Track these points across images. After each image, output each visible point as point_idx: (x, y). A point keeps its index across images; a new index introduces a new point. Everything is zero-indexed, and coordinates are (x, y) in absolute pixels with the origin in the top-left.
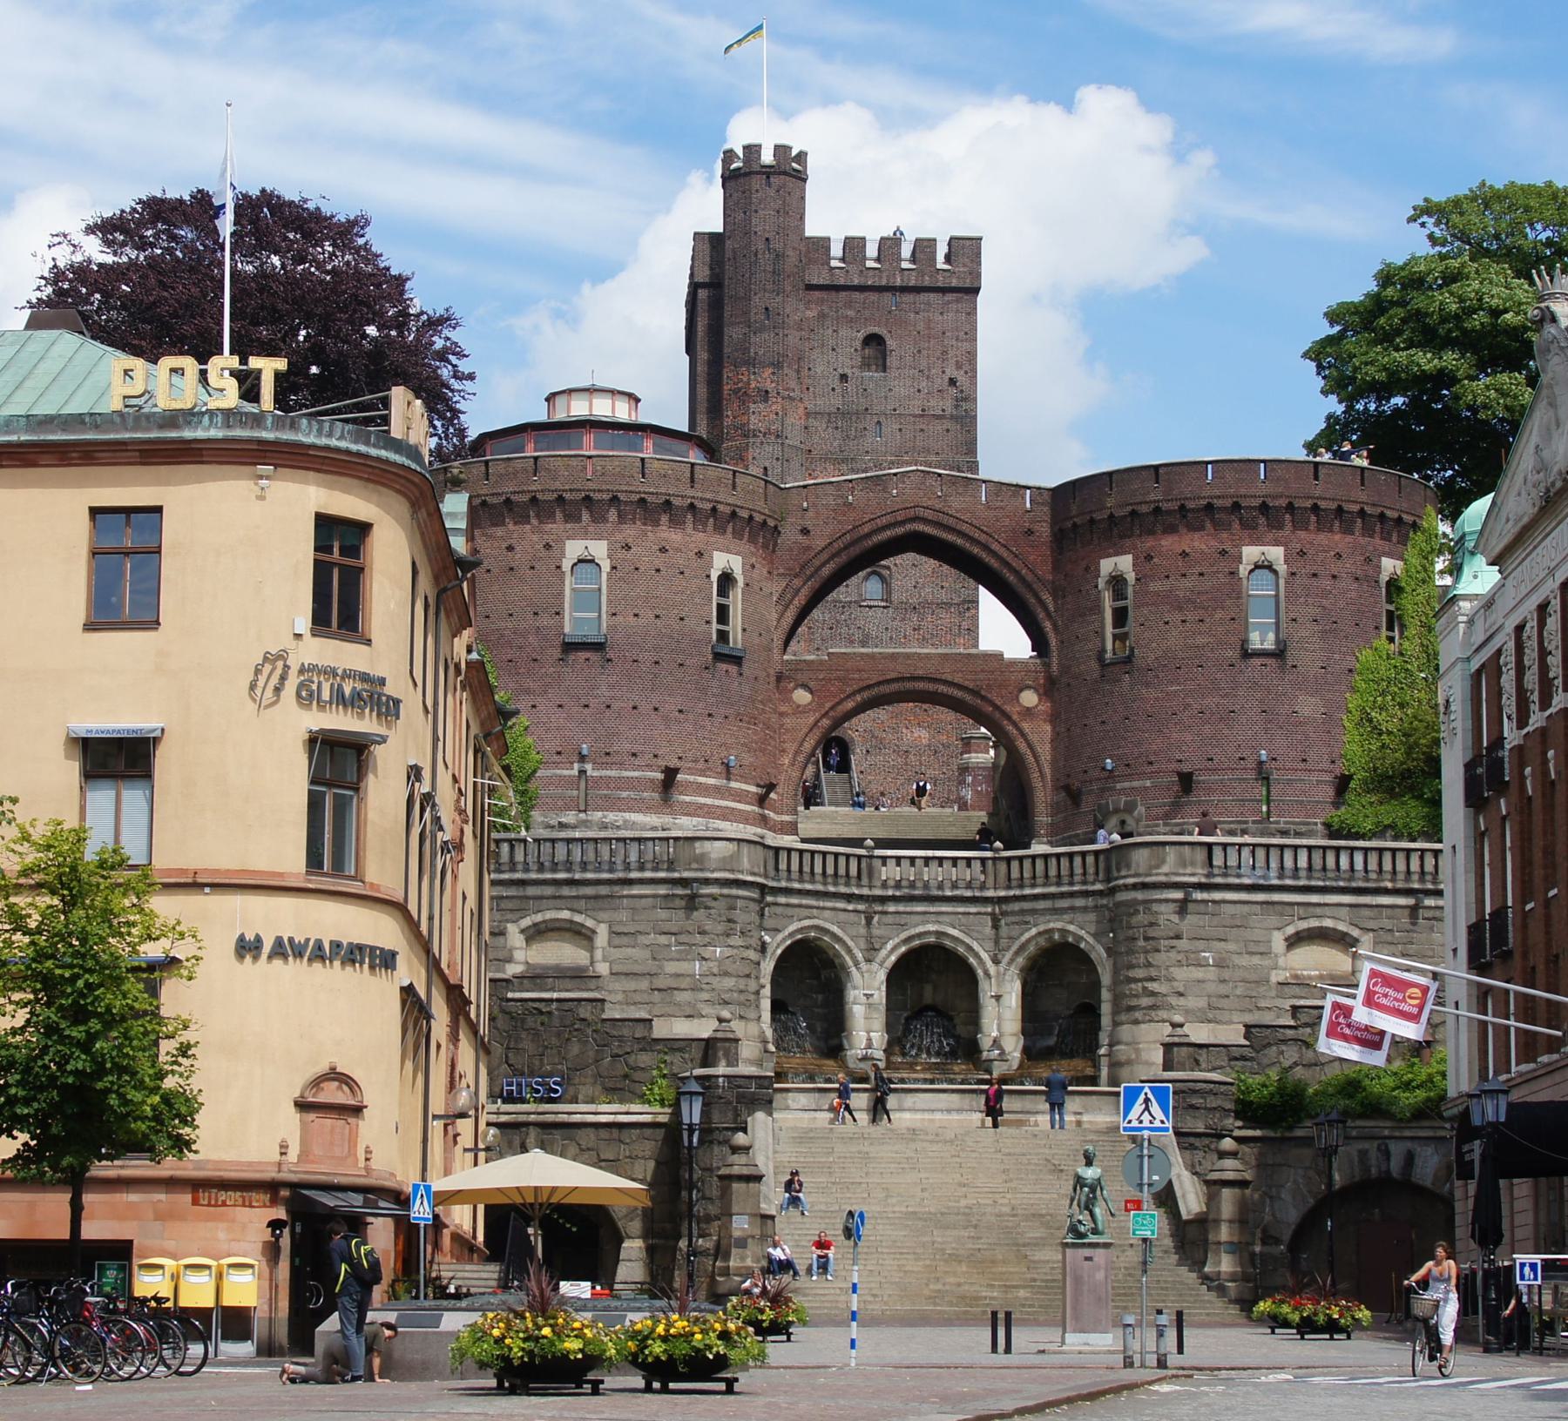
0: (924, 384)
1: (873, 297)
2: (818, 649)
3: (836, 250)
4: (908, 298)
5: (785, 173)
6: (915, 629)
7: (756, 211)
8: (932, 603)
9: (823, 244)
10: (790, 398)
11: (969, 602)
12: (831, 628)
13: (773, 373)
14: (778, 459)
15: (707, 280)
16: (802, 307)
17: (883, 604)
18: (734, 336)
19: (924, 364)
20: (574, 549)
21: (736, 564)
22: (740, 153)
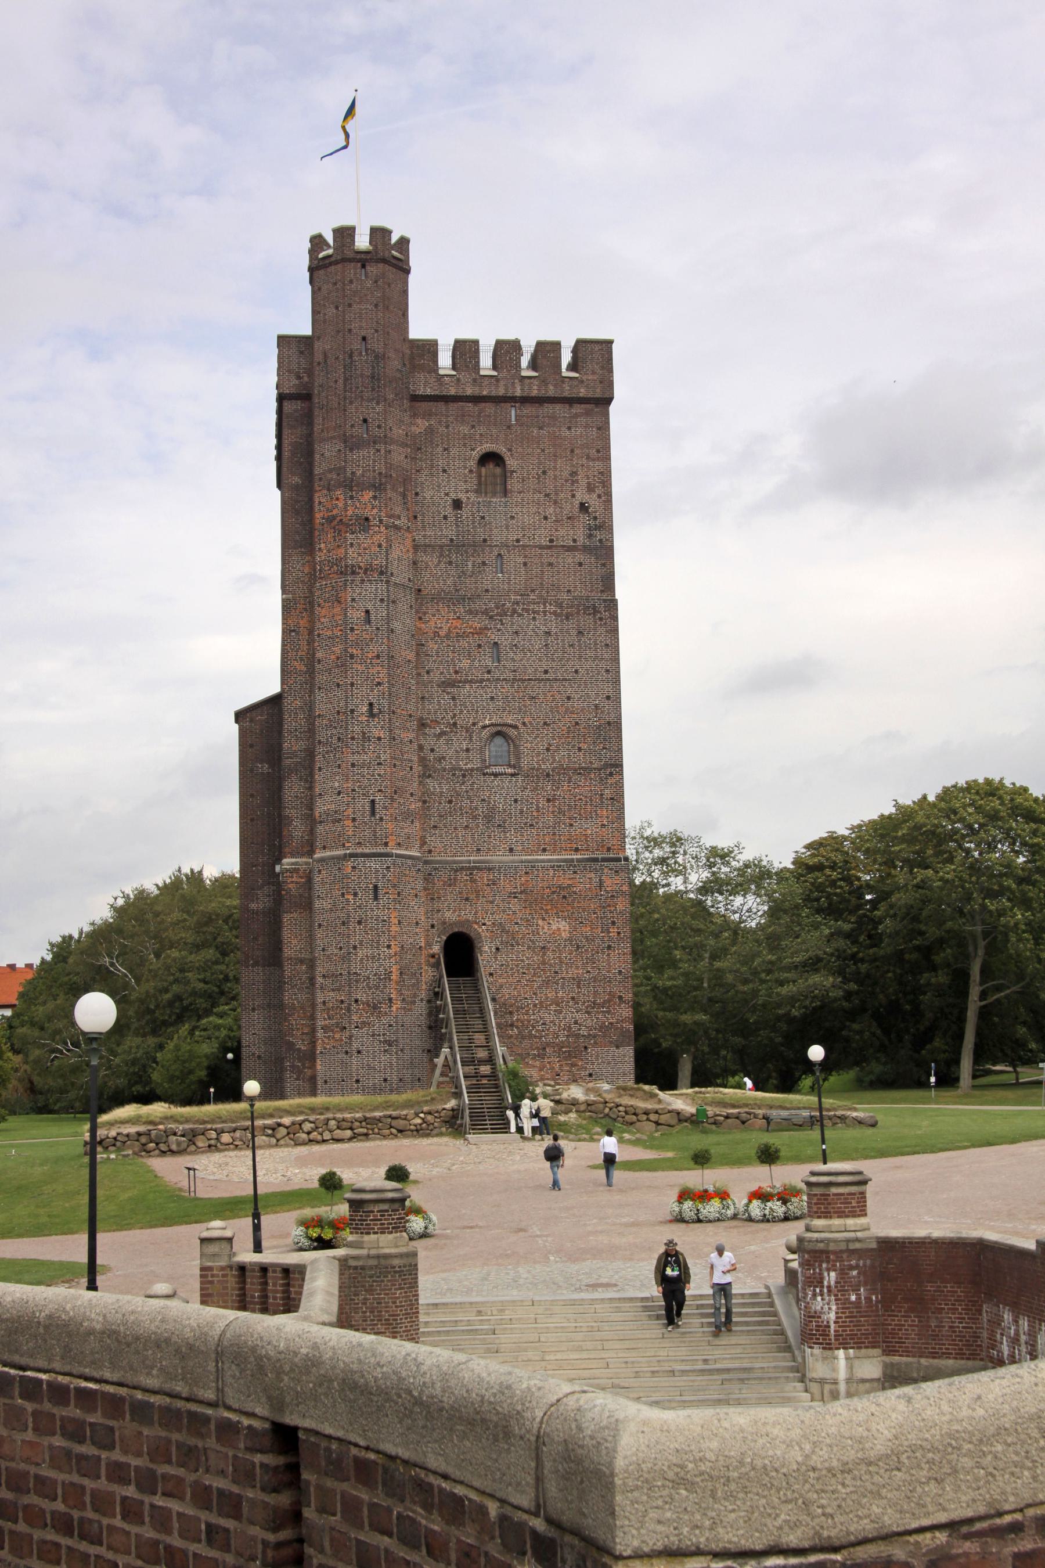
0: (551, 510)
1: (489, 408)
2: (435, 827)
3: (445, 360)
4: (528, 410)
5: (384, 261)
6: (549, 800)
7: (350, 305)
8: (569, 768)
9: (430, 348)
10: (397, 528)
11: (612, 766)
12: (450, 802)
13: (375, 497)
14: (382, 600)
15: (293, 391)
16: (407, 419)
17: (510, 771)
18: (327, 454)
19: (550, 488)
22: (330, 239)
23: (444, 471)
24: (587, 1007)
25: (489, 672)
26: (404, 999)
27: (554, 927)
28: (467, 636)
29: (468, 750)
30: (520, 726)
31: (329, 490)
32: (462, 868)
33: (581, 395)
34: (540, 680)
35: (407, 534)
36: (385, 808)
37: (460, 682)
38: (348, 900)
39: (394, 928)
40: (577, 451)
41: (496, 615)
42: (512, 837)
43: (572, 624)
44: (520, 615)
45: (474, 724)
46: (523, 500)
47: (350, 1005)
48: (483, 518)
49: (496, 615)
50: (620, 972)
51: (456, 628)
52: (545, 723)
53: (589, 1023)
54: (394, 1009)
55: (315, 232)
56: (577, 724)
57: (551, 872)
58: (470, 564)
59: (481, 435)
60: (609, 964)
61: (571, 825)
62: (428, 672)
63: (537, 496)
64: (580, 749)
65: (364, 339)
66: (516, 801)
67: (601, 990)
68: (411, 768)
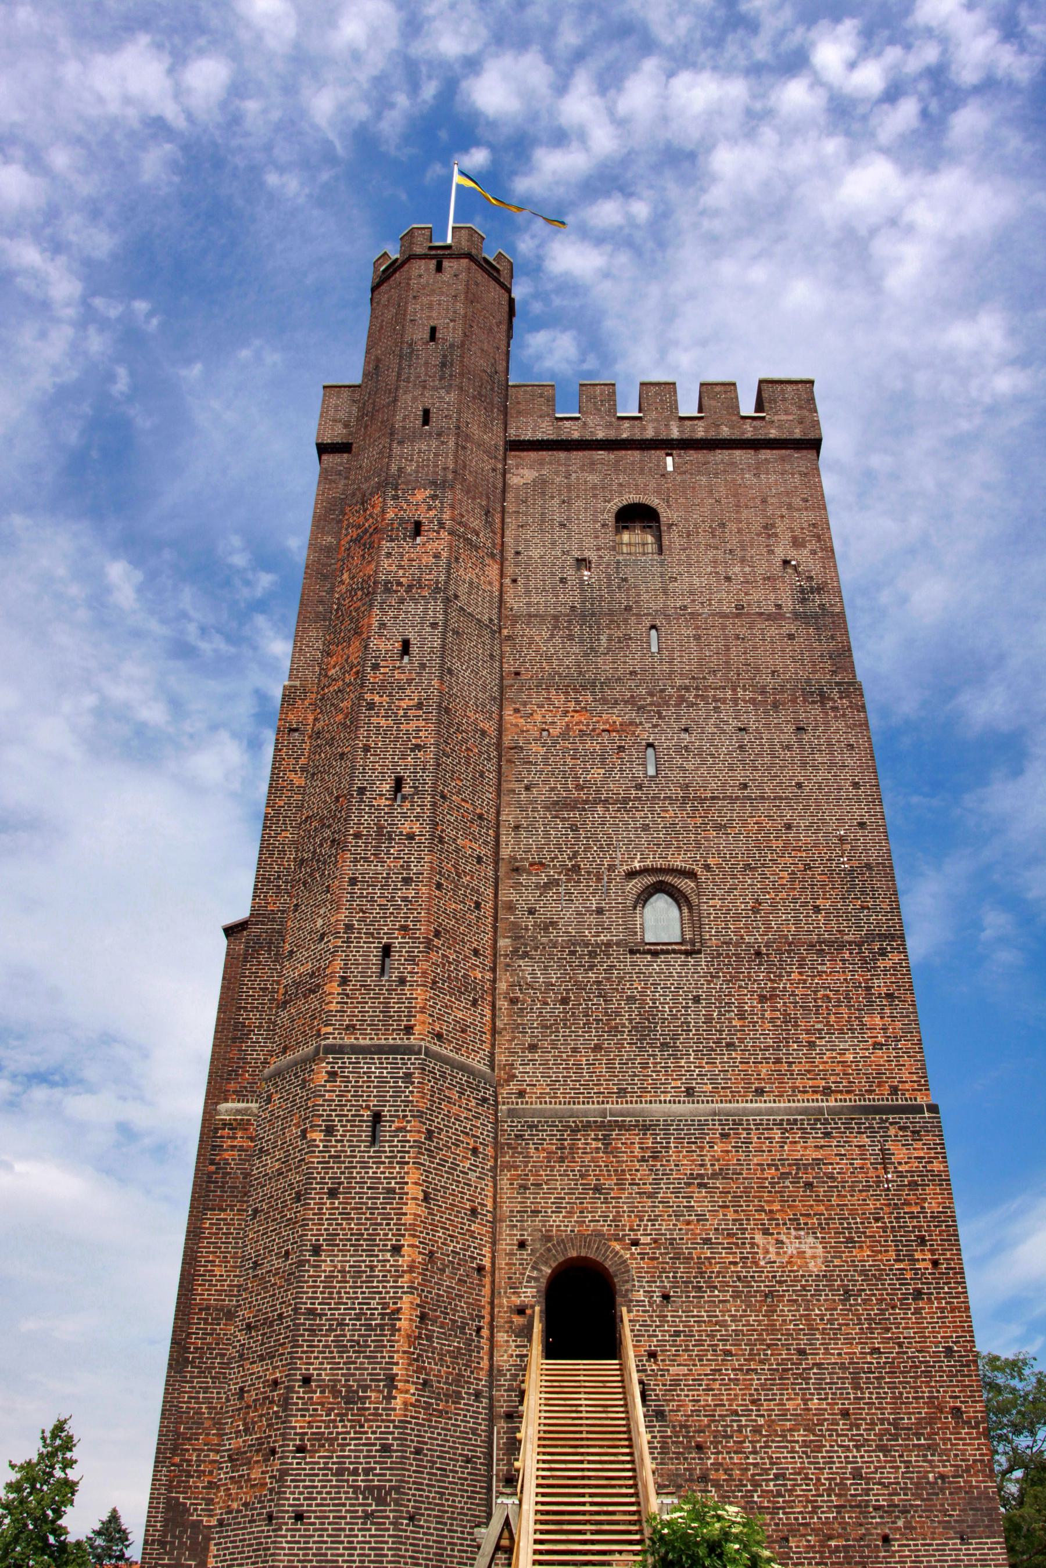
0: (737, 569)
2: (533, 1048)
4: (692, 456)
6: (762, 999)
11: (883, 937)
13: (434, 497)
14: (434, 625)
19: (734, 542)
23: (563, 525)
24: (880, 1436)
25: (639, 787)
26: (426, 1383)
27: (791, 1250)
28: (599, 735)
29: (600, 911)
30: (699, 871)
31: (363, 504)
32: (587, 1126)
33: (772, 436)
34: (733, 799)
35: (487, 561)
36: (412, 960)
37: (586, 802)
38: (312, 1144)
39: (410, 1208)
40: (770, 500)
41: (651, 704)
43: (784, 719)
44: (693, 704)
45: (611, 868)
46: (688, 556)
47: (290, 1389)
48: (625, 580)
49: (651, 704)
50: (949, 1351)
51: (577, 724)
52: (747, 867)
53: (889, 1475)
54: (398, 1403)
56: (807, 867)
57: (777, 1134)
58: (604, 638)
59: (620, 485)
60: (921, 1332)
62: (527, 788)
63: (711, 554)
64: (817, 909)
65: (433, 330)
66: (697, 1000)
67: (908, 1394)
68: (478, 906)
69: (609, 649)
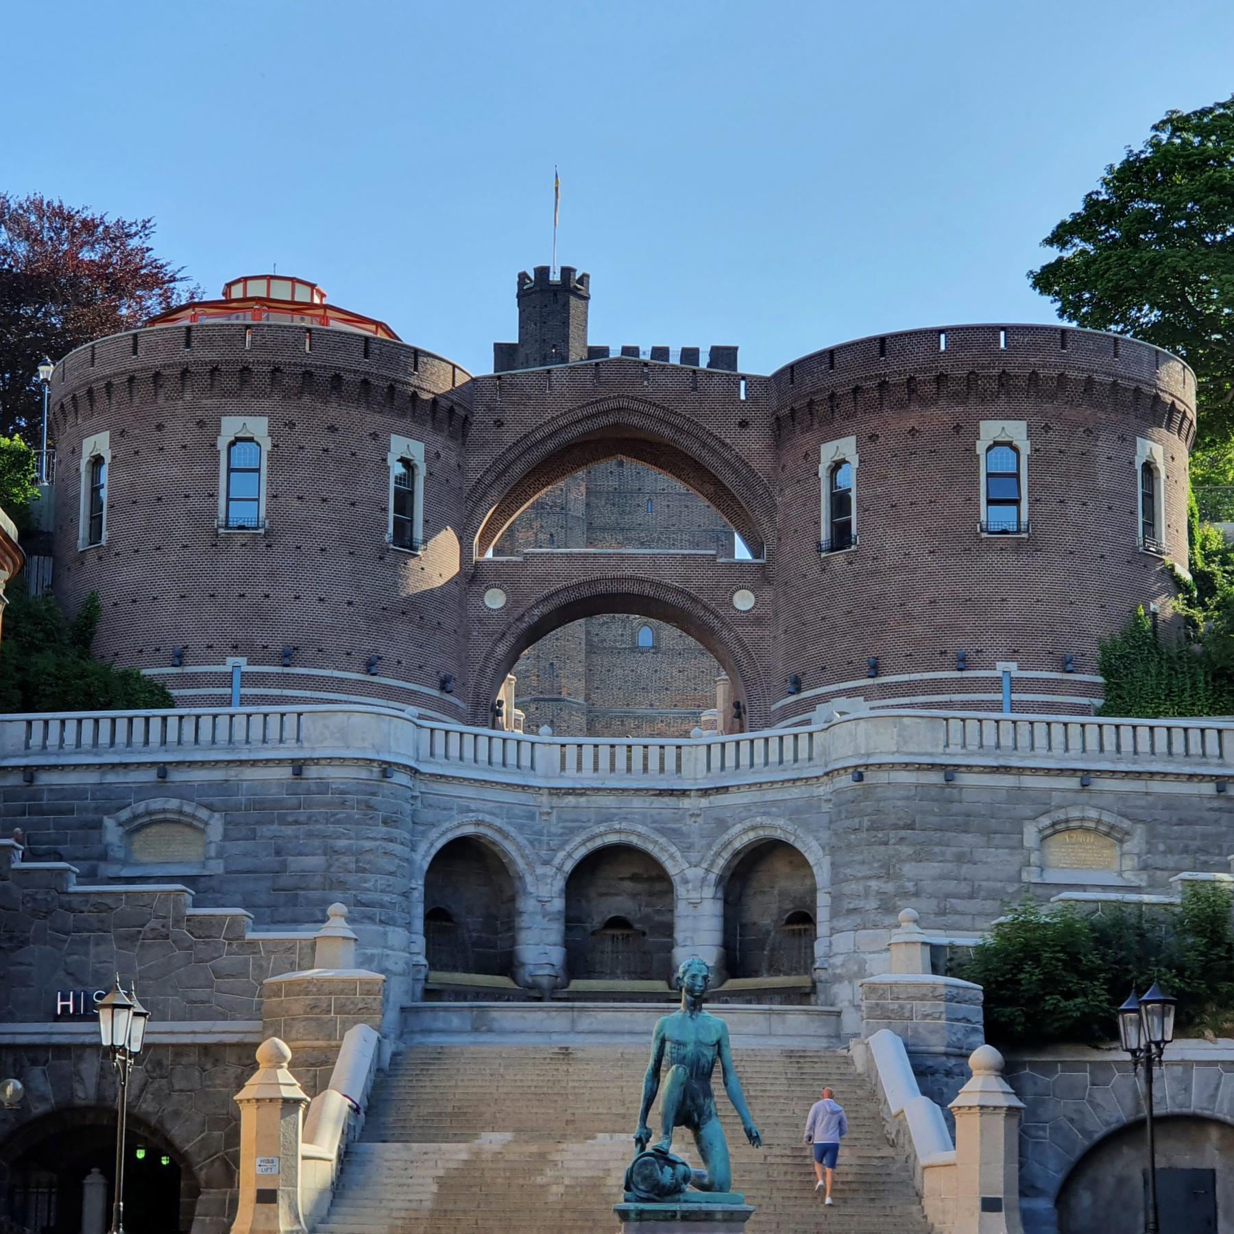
7: (545, 323)
12: (609, 671)
20: (231, 426)
21: (417, 451)
29: (622, 635)
32: (616, 716)
42: (652, 696)
48: (639, 473)
55: (521, 271)
61: (695, 689)
66: (656, 671)
69: (630, 512)
